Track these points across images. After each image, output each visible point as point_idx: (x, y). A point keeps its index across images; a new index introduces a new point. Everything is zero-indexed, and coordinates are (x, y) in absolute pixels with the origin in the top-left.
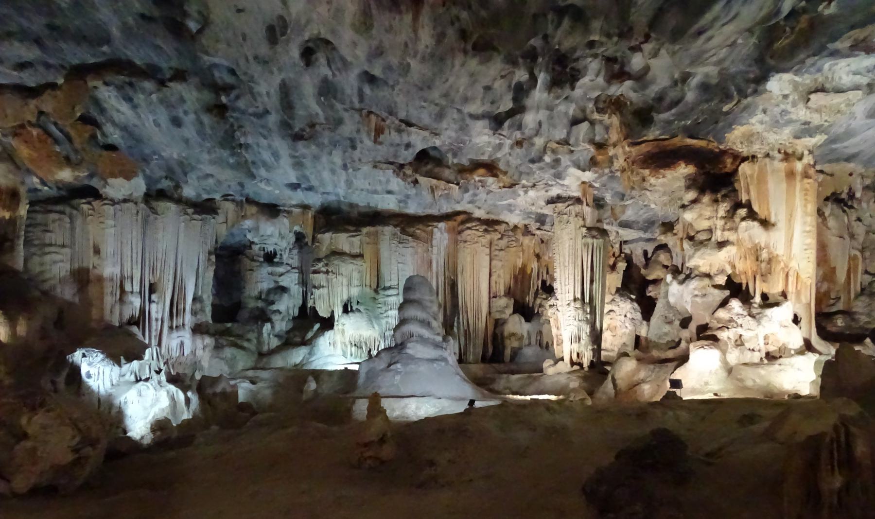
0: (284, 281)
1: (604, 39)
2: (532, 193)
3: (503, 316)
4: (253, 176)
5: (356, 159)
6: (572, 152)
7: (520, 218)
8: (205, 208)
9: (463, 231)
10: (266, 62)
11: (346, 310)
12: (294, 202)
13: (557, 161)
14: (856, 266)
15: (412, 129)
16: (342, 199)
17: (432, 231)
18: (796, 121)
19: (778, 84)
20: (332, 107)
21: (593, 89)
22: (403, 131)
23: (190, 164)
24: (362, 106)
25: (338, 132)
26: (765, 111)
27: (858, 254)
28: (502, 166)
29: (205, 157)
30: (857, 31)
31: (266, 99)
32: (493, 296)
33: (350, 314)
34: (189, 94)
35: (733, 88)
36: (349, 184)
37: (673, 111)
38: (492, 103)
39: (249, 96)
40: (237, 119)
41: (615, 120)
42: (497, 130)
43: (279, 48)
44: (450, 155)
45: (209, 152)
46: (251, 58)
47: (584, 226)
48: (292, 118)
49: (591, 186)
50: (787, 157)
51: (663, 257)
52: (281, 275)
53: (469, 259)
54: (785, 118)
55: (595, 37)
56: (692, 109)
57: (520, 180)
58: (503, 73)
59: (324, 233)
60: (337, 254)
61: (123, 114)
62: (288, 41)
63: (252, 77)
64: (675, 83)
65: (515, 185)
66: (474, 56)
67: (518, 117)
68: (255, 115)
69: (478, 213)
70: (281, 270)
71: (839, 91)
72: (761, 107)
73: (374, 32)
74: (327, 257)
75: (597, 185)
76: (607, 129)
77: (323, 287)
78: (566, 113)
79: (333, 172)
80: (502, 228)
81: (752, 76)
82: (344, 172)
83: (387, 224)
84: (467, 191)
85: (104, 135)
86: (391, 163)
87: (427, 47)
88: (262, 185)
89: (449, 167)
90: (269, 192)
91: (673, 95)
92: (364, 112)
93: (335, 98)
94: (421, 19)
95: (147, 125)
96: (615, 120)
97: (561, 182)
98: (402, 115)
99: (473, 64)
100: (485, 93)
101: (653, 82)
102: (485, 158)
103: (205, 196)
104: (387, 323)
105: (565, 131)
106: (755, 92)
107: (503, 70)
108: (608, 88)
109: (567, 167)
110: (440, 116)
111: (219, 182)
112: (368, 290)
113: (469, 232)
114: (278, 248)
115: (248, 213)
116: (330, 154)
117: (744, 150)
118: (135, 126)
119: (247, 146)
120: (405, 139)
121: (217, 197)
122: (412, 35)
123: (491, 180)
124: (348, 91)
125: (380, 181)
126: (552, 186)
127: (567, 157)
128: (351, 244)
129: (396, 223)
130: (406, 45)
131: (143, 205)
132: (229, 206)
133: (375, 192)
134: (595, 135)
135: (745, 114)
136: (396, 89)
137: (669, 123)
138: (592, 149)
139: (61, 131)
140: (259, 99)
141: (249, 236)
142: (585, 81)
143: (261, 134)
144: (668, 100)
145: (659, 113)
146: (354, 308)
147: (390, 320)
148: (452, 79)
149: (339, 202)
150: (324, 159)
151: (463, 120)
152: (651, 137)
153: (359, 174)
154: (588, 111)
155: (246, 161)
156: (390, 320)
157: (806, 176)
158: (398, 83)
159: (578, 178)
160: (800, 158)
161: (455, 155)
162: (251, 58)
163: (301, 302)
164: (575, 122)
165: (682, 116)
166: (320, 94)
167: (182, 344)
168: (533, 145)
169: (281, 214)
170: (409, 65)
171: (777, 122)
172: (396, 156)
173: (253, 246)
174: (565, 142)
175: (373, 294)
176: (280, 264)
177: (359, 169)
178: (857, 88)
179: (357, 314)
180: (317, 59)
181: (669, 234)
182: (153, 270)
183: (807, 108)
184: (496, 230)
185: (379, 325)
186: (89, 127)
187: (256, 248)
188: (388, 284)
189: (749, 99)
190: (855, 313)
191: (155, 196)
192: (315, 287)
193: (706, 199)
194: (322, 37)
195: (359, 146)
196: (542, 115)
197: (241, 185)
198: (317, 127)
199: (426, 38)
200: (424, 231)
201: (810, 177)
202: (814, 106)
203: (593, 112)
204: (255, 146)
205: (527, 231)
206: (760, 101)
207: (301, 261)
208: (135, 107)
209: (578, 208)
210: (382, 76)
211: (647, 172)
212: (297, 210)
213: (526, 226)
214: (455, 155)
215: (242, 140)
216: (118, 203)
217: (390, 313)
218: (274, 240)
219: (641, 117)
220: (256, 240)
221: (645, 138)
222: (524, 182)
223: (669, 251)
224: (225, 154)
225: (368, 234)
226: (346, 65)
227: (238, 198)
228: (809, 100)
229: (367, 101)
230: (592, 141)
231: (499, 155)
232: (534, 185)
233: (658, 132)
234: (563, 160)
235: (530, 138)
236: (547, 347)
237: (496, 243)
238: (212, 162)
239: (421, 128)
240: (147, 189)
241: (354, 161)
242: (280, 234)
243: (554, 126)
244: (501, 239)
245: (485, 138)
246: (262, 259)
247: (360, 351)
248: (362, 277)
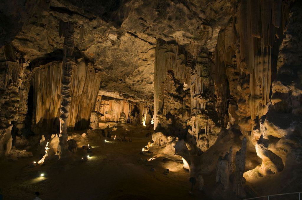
59: (103, 100)
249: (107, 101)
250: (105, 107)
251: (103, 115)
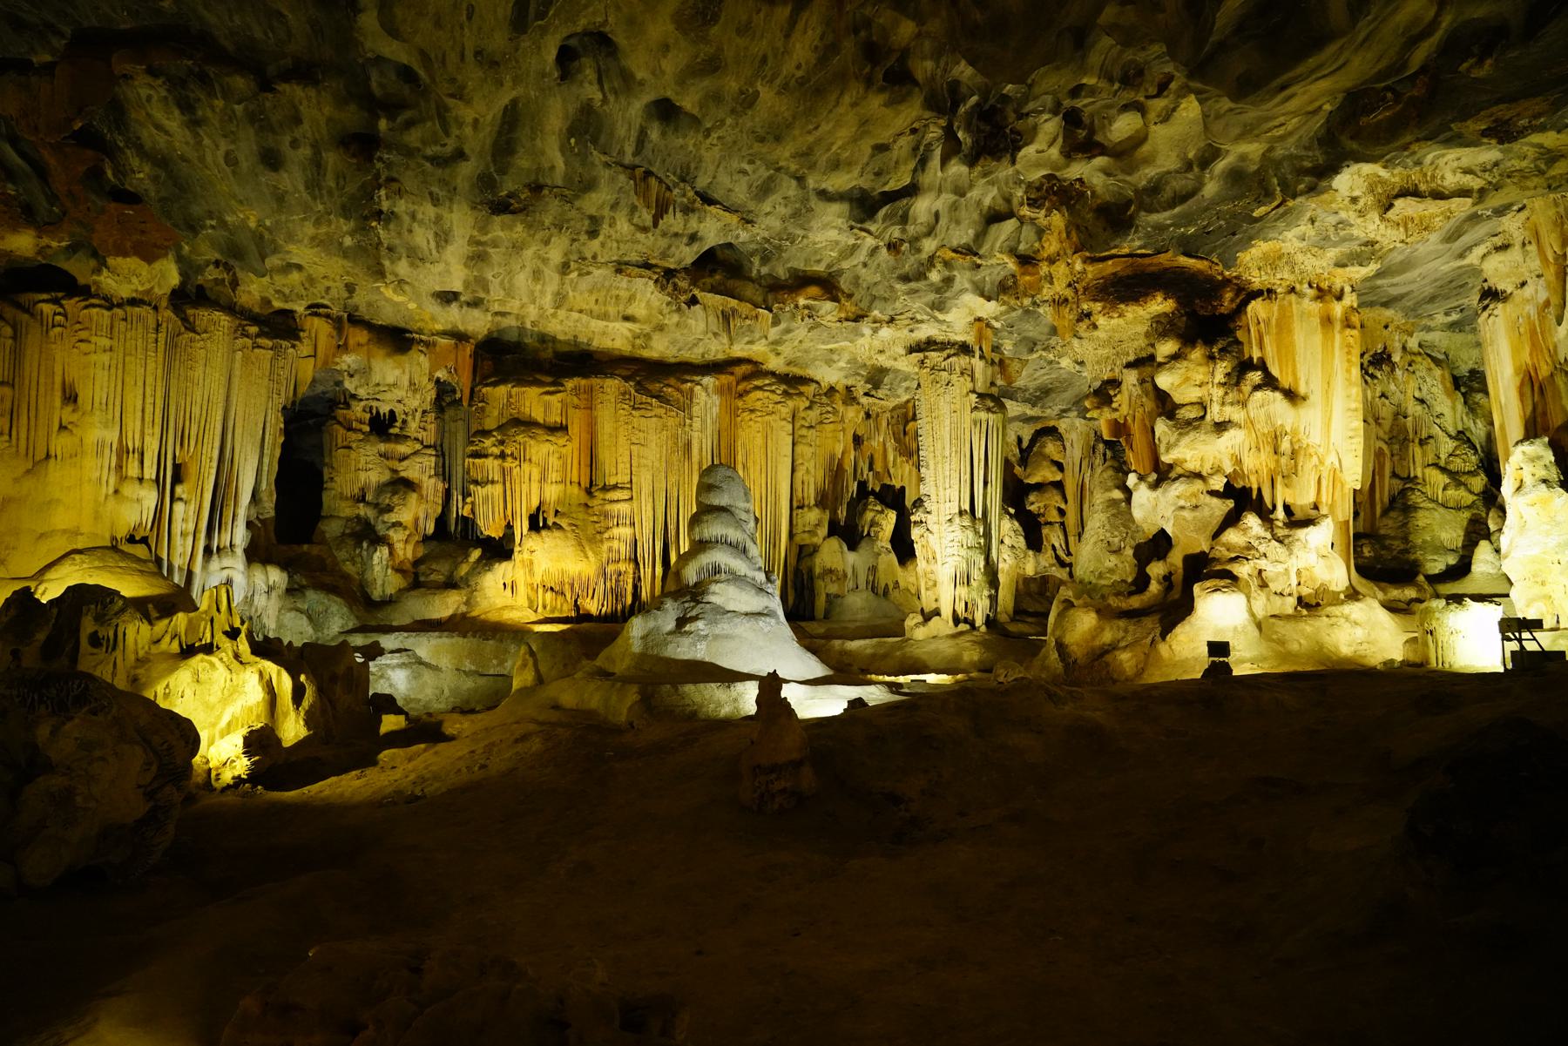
0: (411, 471)
1: (1103, 84)
2: (886, 332)
3: (815, 540)
4: (380, 273)
5: (589, 255)
6: (979, 266)
7: (843, 373)
8: (279, 326)
9: (747, 392)
10: (494, 64)
11: (536, 523)
12: (439, 327)
13: (948, 281)
14: (1382, 467)
15: (712, 208)
16: (528, 326)
17: (692, 390)
18: (1357, 238)
19: (1350, 181)
20: (584, 157)
21: (1038, 165)
22: (693, 211)
23: (274, 241)
24: (637, 161)
25: (577, 203)
26: (1313, 221)
27: (1385, 447)
28: (844, 283)
29: (309, 229)
30: (1501, 106)
31: (468, 130)
32: (796, 506)
33: (544, 533)
34: (317, 109)
35: (1275, 181)
36: (560, 300)
37: (1177, 210)
38: (878, 174)
39: (432, 126)
40: (389, 165)
41: (1058, 220)
42: (862, 221)
43: (525, 43)
44: (756, 261)
45: (317, 223)
46: (469, 54)
47: (973, 391)
48: (503, 171)
49: (988, 325)
50: (1322, 294)
51: (1051, 448)
52: (404, 458)
53: (759, 441)
54: (1342, 233)
55: (1089, 80)
56: (1206, 209)
57: (870, 309)
58: (916, 125)
59: (495, 384)
60: (526, 424)
61: (167, 133)
62: (544, 31)
63: (463, 87)
64: (1188, 166)
65: (863, 317)
66: (881, 90)
67: (905, 201)
68: (433, 160)
69: (775, 364)
70: (403, 449)
71: (1438, 195)
72: (1308, 215)
73: (715, 30)
74: (500, 428)
75: (997, 325)
76: (1040, 233)
77: (493, 482)
78: (979, 203)
79: (537, 275)
80: (810, 389)
81: (1307, 164)
82: (556, 277)
83: (612, 375)
84: (776, 322)
85: (121, 171)
86: (647, 266)
87: (798, 67)
88: (389, 293)
89: (753, 281)
90: (397, 304)
91: (1177, 184)
92: (639, 172)
93: (595, 141)
94: (805, 15)
95: (209, 159)
96: (1058, 220)
97: (941, 317)
98: (702, 182)
99: (875, 103)
100: (872, 156)
101: (1148, 161)
102: (821, 268)
103: (277, 304)
104: (610, 550)
105: (971, 232)
106: (1312, 190)
107: (919, 119)
108: (1068, 166)
109: (962, 291)
110: (765, 190)
111: (311, 280)
112: (575, 490)
113: (759, 394)
114: (398, 409)
115: (351, 342)
116: (547, 242)
117: (1257, 280)
118: (183, 159)
119: (386, 217)
120: (693, 224)
121: (299, 308)
122: (779, 44)
123: (828, 306)
124: (621, 131)
125: (617, 297)
126: (922, 321)
127: (968, 274)
128: (547, 407)
129: (625, 373)
130: (764, 60)
131: (169, 313)
132: (320, 328)
133: (604, 317)
134: (1019, 242)
135: (1281, 224)
136: (715, 135)
137: (1160, 228)
138: (1012, 265)
139: (22, 155)
140: (455, 131)
141: (349, 385)
142: (1028, 152)
143: (431, 194)
144: (1167, 194)
145: (1151, 211)
146: (550, 523)
147: (615, 544)
148: (825, 128)
149: (522, 330)
150: (528, 253)
151: (805, 200)
152: (1126, 251)
153: (584, 284)
154: (1015, 202)
155: (380, 243)
156: (615, 544)
157: (1348, 325)
158: (723, 122)
159: (971, 312)
160: (1339, 297)
161: (765, 260)
162: (469, 54)
163: (439, 510)
164: (994, 217)
165: (1188, 219)
166: (572, 131)
167: (229, 582)
168: (919, 251)
169: (415, 348)
170: (757, 94)
171: (1327, 238)
172: (664, 255)
173: (353, 403)
174: (969, 251)
175: (583, 498)
176: (401, 438)
177: (589, 273)
178: (1464, 193)
179: (557, 533)
180: (579, 70)
181: (1106, 409)
182: (182, 439)
183: (1382, 219)
184: (801, 394)
185: (596, 554)
186: (90, 153)
187: (358, 409)
188: (612, 481)
189: (1299, 200)
190: (1385, 537)
191: (188, 298)
192: (476, 483)
193: (1197, 354)
194: (607, 29)
195: (605, 229)
196: (942, 203)
197: (350, 288)
198: (546, 192)
199: (802, 50)
200: (678, 390)
201: (1353, 327)
202: (1395, 218)
203: (1022, 204)
204: (407, 219)
205: (850, 397)
206: (1310, 205)
207: (441, 432)
208: (194, 124)
209: (962, 361)
210: (695, 111)
211: (1098, 306)
212: (444, 342)
213: (848, 388)
214: (765, 260)
215: (385, 205)
216: (119, 306)
217: (616, 531)
218: (400, 394)
219: (1115, 217)
220: (362, 392)
221: (1114, 251)
222: (876, 313)
223: (1060, 438)
224: (346, 226)
225: (576, 391)
226: (628, 83)
227: (335, 311)
228: (1391, 206)
229: (647, 152)
230: (1013, 252)
231: (845, 265)
232: (892, 320)
233: (1137, 243)
234: (958, 279)
235: (917, 239)
236: (886, 593)
237: (802, 414)
238: (316, 241)
239: (727, 209)
240: (183, 284)
241: (584, 259)
242: (412, 384)
243: (958, 222)
244: (809, 408)
245: (833, 234)
246: (367, 428)
247: (560, 598)
248: (564, 465)
249: (532, 392)
250: (520, 458)
251: (500, 550)
